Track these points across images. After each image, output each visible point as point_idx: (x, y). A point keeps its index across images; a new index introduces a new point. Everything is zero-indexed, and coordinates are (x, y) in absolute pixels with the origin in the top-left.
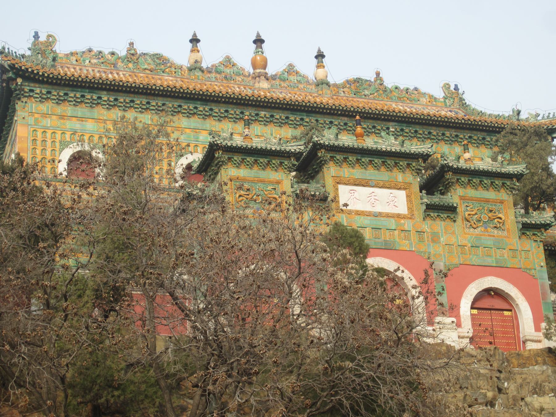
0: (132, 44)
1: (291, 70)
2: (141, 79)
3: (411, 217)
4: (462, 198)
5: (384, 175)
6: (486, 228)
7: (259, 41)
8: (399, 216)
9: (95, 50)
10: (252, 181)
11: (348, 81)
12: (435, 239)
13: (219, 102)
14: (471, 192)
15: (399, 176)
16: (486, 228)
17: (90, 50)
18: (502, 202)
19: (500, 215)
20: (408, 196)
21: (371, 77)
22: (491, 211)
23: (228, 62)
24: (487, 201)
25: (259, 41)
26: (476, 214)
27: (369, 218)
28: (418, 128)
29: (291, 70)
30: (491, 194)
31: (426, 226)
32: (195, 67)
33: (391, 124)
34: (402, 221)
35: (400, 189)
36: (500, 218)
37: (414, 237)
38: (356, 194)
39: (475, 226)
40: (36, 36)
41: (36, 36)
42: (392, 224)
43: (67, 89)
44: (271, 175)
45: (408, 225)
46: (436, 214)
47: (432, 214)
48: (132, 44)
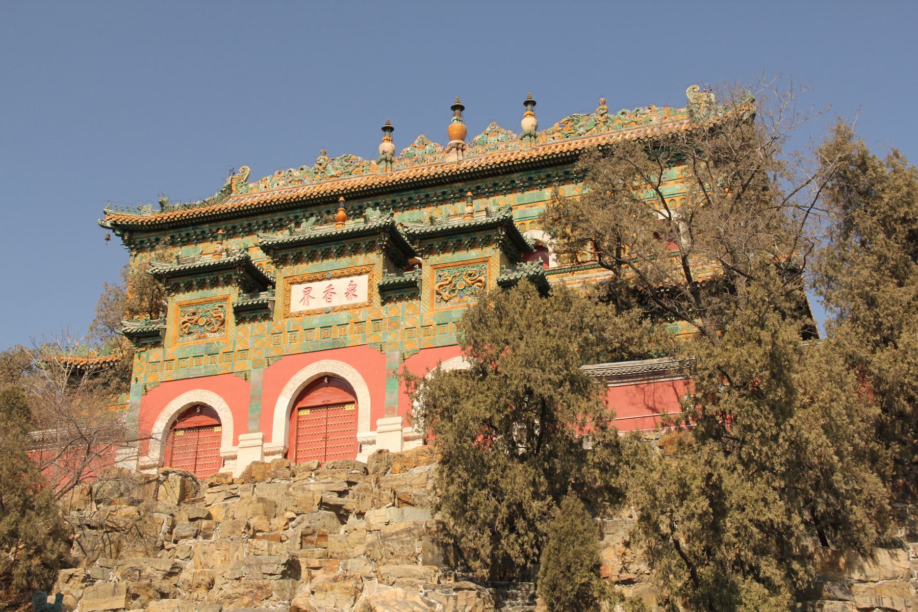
4: (435, 267)
5: (344, 262)
6: (461, 297)
8: (356, 307)
10: (200, 304)
12: (394, 323)
13: (319, 204)
15: (361, 259)
16: (461, 297)
18: (485, 260)
19: (482, 278)
20: (370, 280)
22: (470, 275)
24: (466, 263)
26: (451, 282)
27: (319, 316)
30: (474, 254)
33: (515, 175)
35: (361, 274)
36: (480, 281)
37: (369, 327)
39: (446, 298)
42: (344, 317)
43: (172, 231)
44: (218, 292)
45: (362, 315)
46: (398, 295)
47: (393, 295)
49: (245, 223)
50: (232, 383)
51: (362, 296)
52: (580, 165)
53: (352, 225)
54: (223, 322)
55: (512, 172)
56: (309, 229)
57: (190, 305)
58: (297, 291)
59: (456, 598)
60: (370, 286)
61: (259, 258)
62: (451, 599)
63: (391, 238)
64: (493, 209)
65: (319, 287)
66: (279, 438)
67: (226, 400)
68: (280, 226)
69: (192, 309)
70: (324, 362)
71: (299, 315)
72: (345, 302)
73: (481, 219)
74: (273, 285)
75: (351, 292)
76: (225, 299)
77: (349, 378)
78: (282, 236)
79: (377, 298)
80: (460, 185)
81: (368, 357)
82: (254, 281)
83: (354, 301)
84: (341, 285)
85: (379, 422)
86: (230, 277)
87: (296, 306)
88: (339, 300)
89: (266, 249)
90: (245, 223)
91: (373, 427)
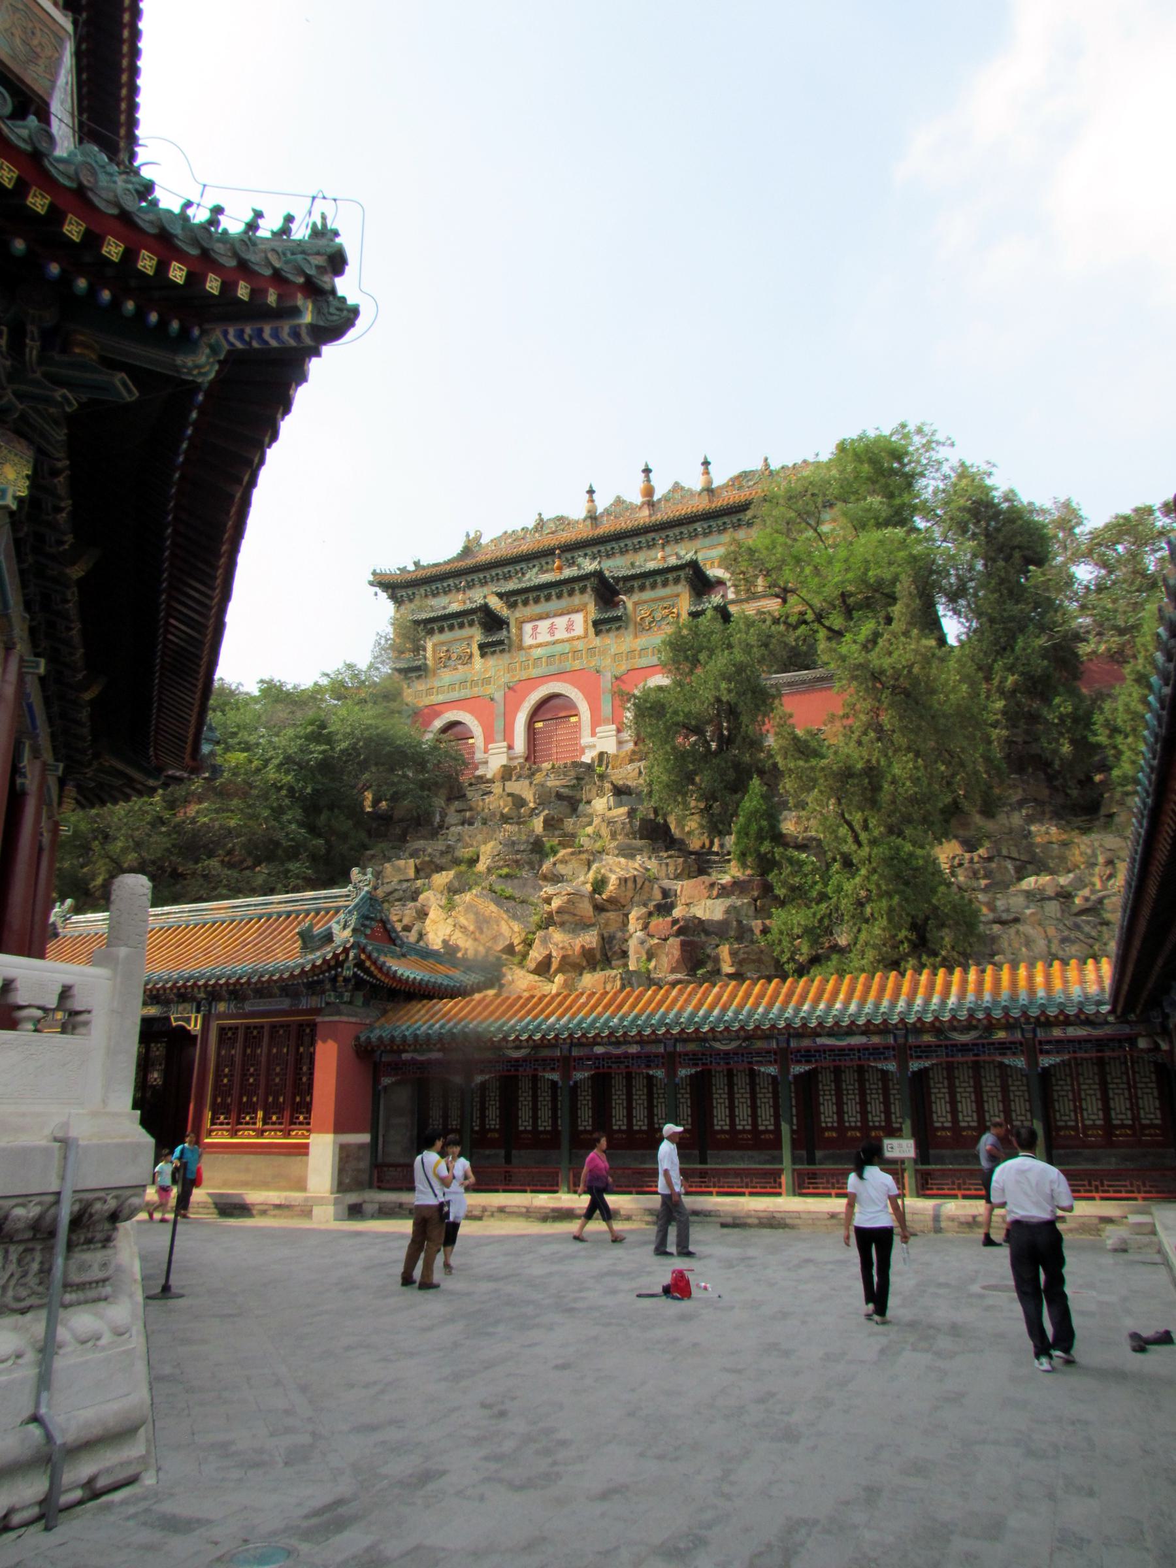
0: (540, 515)
1: (677, 487)
2: (548, 541)
3: (586, 636)
5: (564, 603)
7: (647, 471)
9: (510, 531)
11: (731, 480)
12: (604, 652)
14: (648, 595)
15: (577, 599)
17: (506, 533)
21: (758, 465)
23: (619, 501)
24: (662, 599)
25: (647, 471)
28: (726, 519)
29: (677, 487)
30: (668, 591)
31: (597, 641)
32: (709, 490)
34: (576, 643)
35: (577, 611)
38: (539, 630)
40: (468, 535)
41: (468, 535)
42: (566, 647)
44: (467, 632)
45: (580, 645)
48: (540, 515)
49: (481, 576)
50: (479, 705)
51: (579, 630)
52: (749, 514)
53: (568, 573)
54: (471, 656)
55: (694, 522)
56: (535, 577)
57: (443, 644)
58: (528, 628)
59: (667, 864)
60: (586, 621)
61: (495, 603)
62: (664, 867)
63: (694, 573)
64: (682, 553)
65: (544, 625)
66: (520, 745)
67: (477, 718)
68: (507, 577)
69: (445, 648)
70: (551, 684)
71: (531, 647)
72: (565, 635)
73: (673, 561)
74: (508, 624)
75: (569, 628)
76: (471, 637)
77: (572, 696)
78: (511, 585)
79: (591, 631)
80: (652, 535)
81: (587, 681)
82: (492, 622)
83: (573, 634)
84: (561, 622)
85: (598, 730)
86: (473, 620)
87: (528, 641)
88: (561, 634)
89: (500, 595)
90: (481, 576)
91: (593, 734)
